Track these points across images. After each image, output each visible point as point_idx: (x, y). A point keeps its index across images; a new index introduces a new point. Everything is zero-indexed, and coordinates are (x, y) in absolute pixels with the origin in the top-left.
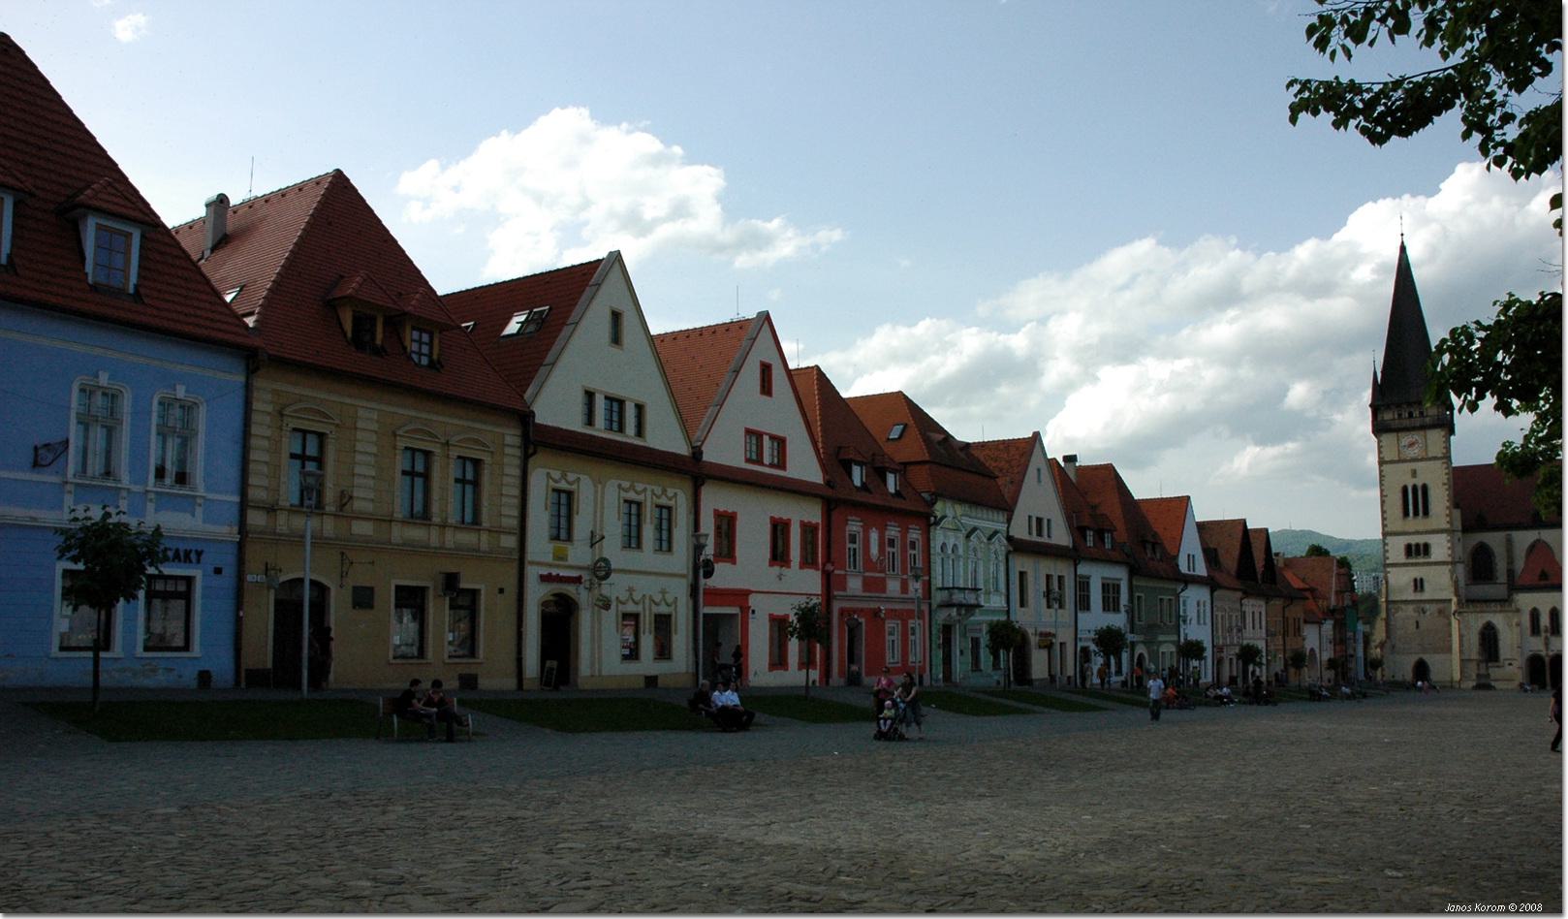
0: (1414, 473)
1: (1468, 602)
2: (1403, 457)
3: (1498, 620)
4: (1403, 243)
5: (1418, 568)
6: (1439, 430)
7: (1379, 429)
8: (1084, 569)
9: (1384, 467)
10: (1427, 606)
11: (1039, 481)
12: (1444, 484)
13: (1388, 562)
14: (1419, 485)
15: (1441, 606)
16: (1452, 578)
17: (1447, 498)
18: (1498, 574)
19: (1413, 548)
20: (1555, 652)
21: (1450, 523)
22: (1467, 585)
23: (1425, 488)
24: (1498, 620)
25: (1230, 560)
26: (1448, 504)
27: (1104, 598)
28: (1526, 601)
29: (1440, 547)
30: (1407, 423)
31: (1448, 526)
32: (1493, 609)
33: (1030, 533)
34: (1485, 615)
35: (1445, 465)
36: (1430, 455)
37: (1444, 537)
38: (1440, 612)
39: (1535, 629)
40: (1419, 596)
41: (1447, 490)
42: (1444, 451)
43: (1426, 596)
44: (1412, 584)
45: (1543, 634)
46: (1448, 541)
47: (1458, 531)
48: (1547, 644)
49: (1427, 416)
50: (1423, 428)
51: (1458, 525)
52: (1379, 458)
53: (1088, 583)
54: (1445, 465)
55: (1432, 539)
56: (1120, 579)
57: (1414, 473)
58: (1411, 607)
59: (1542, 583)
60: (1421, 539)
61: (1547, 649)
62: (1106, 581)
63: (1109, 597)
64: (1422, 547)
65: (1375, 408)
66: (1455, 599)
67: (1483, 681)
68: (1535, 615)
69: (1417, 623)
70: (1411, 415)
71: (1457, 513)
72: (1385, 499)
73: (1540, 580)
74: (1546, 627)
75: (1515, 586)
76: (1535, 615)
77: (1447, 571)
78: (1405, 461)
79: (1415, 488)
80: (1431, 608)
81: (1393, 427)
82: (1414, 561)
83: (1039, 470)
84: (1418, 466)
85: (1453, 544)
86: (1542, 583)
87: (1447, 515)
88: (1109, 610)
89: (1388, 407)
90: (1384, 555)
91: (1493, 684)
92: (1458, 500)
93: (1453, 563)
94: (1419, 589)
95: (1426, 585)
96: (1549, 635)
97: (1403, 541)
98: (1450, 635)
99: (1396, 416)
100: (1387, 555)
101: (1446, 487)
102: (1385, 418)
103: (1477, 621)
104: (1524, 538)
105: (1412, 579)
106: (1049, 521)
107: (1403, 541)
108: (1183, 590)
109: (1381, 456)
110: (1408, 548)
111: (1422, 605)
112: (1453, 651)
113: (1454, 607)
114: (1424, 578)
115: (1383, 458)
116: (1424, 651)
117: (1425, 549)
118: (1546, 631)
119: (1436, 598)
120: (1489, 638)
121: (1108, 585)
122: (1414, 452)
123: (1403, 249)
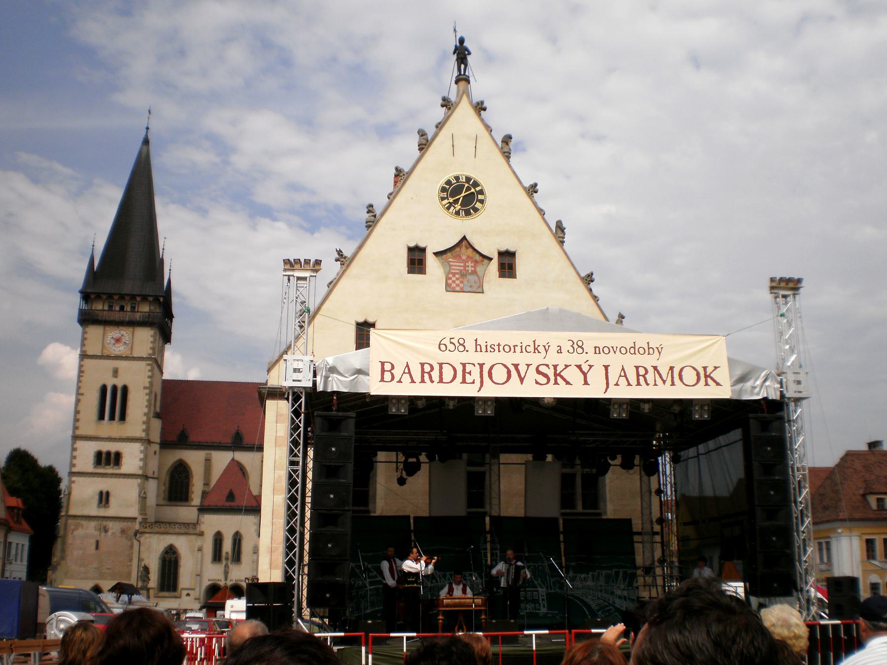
0: (116, 372)
2: (106, 353)
3: (182, 543)
4: (147, 135)
5: (104, 479)
6: (149, 329)
7: (86, 319)
9: (88, 362)
10: (110, 524)
12: (145, 388)
15: (124, 524)
16: (139, 496)
18: (193, 496)
19: (104, 456)
20: (234, 582)
21: (147, 430)
22: (157, 505)
23: (125, 389)
24: (182, 543)
26: (146, 410)
28: (213, 523)
30: (117, 316)
31: (143, 435)
32: (177, 530)
34: (168, 537)
35: (149, 368)
37: (137, 447)
38: (123, 531)
39: (217, 556)
40: (102, 512)
41: (147, 394)
42: (151, 352)
43: (111, 512)
44: (97, 498)
45: (224, 562)
46: (141, 452)
47: (157, 443)
48: (226, 573)
49: (138, 311)
50: (132, 324)
51: (156, 436)
52: (82, 351)
54: (149, 368)
57: (116, 372)
58: (93, 524)
59: (228, 504)
60: (112, 447)
61: (226, 579)
64: (113, 456)
65: (86, 296)
66: (140, 519)
68: (218, 539)
70: (122, 308)
71: (157, 424)
73: (227, 501)
74: (227, 553)
75: (204, 509)
76: (218, 539)
78: (108, 357)
79: (115, 388)
80: (114, 527)
81: (100, 318)
84: (122, 364)
86: (228, 504)
87: (144, 423)
89: (99, 296)
90: (71, 462)
93: (145, 477)
94: (104, 503)
98: (131, 560)
99: (106, 308)
100: (74, 461)
101: (147, 391)
104: (222, 460)
109: (84, 349)
110: (99, 455)
111: (104, 523)
114: (109, 491)
115: (85, 351)
122: (120, 349)
123: (146, 142)
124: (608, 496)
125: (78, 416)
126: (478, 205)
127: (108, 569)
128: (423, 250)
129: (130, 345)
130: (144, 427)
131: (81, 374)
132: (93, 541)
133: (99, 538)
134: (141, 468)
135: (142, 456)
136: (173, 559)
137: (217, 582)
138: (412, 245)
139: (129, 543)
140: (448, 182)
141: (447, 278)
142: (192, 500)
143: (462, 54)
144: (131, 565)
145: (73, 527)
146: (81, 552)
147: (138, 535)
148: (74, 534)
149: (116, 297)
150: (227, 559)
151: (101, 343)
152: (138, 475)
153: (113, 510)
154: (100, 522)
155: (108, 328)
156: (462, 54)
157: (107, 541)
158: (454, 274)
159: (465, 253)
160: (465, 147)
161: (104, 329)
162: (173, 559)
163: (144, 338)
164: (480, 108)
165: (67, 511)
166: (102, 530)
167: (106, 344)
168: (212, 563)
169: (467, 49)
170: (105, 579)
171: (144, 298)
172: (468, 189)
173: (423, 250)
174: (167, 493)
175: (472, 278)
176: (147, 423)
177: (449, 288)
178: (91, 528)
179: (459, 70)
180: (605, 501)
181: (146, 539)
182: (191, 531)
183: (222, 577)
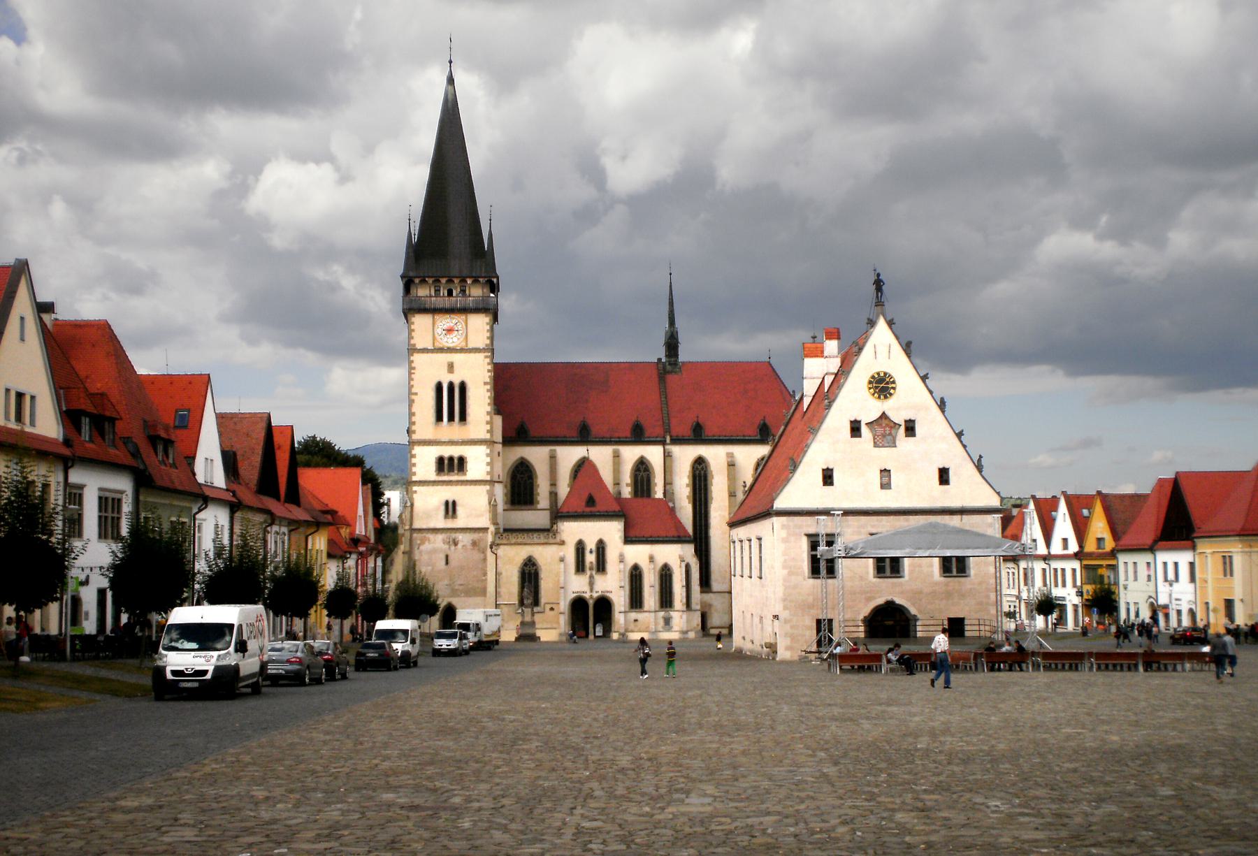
0: (451, 367)
1: (509, 533)
2: (438, 345)
8: (76, 476)
9: (417, 358)
10: (460, 536)
11: (22, 339)
12: (485, 383)
13: (414, 478)
14: (457, 383)
15: (476, 536)
16: (490, 503)
17: (489, 401)
18: (539, 498)
19: (446, 462)
20: (600, 594)
21: (491, 431)
23: (463, 387)
25: (251, 469)
26: (489, 409)
27: (100, 517)
28: (572, 531)
29: (479, 462)
30: (446, 302)
31: (488, 436)
33: (7, 417)
36: (471, 346)
37: (482, 450)
38: (474, 544)
39: (580, 567)
40: (450, 524)
41: (488, 391)
42: (488, 342)
43: (460, 522)
44: (443, 508)
45: (588, 573)
46: (488, 455)
48: (591, 584)
49: (470, 296)
50: (465, 310)
53: (81, 496)
55: (468, 452)
56: (122, 492)
57: (451, 367)
58: (440, 537)
59: (588, 510)
60: (455, 451)
61: (591, 590)
62: (103, 494)
63: (106, 517)
64: (456, 461)
66: (492, 528)
67: (528, 631)
68: (580, 548)
69: (447, 557)
70: (450, 293)
71: (498, 420)
72: (413, 397)
74: (591, 563)
75: (558, 515)
77: (485, 493)
78: (441, 350)
79: (451, 386)
80: (464, 539)
82: (445, 478)
83: (22, 319)
84: (456, 358)
85: (492, 460)
86: (588, 510)
88: (106, 537)
91: (539, 633)
92: (501, 402)
93: (491, 482)
94: (450, 513)
95: (459, 509)
96: (594, 572)
97: (432, 453)
98: (485, 574)
101: (488, 387)
102: (419, 294)
103: (513, 556)
104: (570, 455)
105: (443, 502)
106: (33, 398)
107: (432, 453)
108: (200, 510)
110: (440, 461)
111: (454, 535)
112: (488, 595)
113: (490, 538)
114: (458, 503)
116: (455, 593)
117: (458, 464)
118: (591, 569)
119: (470, 526)
120: (530, 575)
121: (106, 499)
122: (453, 340)
123: (451, 80)
124: (971, 566)
125: (414, 419)
126: (892, 391)
127: (461, 585)
128: (860, 422)
129: (464, 334)
130: (488, 427)
131: (413, 371)
132: (443, 557)
133: (449, 553)
134: (488, 473)
135: (488, 460)
136: (533, 571)
137: (584, 595)
138: (853, 419)
139: (482, 556)
140: (873, 377)
141: (874, 439)
142: (538, 503)
143: (879, 284)
144: (486, 580)
145: (419, 542)
146: (430, 568)
147: (494, 548)
148: (422, 548)
149: (444, 281)
150: (591, 569)
151: (431, 333)
152: (487, 481)
153: (461, 521)
154: (448, 534)
155: (437, 317)
156: (879, 284)
157: (457, 555)
158: (878, 436)
159: (884, 422)
160: (882, 351)
161: (434, 318)
162: (533, 571)
163: (478, 325)
164: (890, 323)
165: (411, 524)
166: (451, 543)
167: (436, 335)
168: (576, 574)
169: (881, 281)
170: (459, 596)
171: (476, 281)
172: (887, 383)
173: (860, 422)
174: (509, 496)
175: (889, 438)
176: (490, 423)
177: (876, 445)
178: (438, 541)
179: (877, 297)
180: (969, 569)
181: (501, 551)
182: (551, 540)
183: (586, 588)
